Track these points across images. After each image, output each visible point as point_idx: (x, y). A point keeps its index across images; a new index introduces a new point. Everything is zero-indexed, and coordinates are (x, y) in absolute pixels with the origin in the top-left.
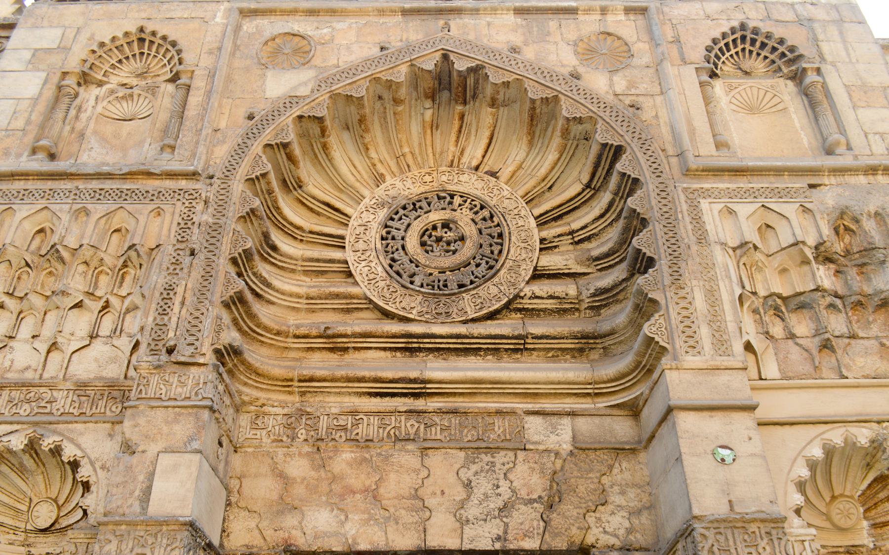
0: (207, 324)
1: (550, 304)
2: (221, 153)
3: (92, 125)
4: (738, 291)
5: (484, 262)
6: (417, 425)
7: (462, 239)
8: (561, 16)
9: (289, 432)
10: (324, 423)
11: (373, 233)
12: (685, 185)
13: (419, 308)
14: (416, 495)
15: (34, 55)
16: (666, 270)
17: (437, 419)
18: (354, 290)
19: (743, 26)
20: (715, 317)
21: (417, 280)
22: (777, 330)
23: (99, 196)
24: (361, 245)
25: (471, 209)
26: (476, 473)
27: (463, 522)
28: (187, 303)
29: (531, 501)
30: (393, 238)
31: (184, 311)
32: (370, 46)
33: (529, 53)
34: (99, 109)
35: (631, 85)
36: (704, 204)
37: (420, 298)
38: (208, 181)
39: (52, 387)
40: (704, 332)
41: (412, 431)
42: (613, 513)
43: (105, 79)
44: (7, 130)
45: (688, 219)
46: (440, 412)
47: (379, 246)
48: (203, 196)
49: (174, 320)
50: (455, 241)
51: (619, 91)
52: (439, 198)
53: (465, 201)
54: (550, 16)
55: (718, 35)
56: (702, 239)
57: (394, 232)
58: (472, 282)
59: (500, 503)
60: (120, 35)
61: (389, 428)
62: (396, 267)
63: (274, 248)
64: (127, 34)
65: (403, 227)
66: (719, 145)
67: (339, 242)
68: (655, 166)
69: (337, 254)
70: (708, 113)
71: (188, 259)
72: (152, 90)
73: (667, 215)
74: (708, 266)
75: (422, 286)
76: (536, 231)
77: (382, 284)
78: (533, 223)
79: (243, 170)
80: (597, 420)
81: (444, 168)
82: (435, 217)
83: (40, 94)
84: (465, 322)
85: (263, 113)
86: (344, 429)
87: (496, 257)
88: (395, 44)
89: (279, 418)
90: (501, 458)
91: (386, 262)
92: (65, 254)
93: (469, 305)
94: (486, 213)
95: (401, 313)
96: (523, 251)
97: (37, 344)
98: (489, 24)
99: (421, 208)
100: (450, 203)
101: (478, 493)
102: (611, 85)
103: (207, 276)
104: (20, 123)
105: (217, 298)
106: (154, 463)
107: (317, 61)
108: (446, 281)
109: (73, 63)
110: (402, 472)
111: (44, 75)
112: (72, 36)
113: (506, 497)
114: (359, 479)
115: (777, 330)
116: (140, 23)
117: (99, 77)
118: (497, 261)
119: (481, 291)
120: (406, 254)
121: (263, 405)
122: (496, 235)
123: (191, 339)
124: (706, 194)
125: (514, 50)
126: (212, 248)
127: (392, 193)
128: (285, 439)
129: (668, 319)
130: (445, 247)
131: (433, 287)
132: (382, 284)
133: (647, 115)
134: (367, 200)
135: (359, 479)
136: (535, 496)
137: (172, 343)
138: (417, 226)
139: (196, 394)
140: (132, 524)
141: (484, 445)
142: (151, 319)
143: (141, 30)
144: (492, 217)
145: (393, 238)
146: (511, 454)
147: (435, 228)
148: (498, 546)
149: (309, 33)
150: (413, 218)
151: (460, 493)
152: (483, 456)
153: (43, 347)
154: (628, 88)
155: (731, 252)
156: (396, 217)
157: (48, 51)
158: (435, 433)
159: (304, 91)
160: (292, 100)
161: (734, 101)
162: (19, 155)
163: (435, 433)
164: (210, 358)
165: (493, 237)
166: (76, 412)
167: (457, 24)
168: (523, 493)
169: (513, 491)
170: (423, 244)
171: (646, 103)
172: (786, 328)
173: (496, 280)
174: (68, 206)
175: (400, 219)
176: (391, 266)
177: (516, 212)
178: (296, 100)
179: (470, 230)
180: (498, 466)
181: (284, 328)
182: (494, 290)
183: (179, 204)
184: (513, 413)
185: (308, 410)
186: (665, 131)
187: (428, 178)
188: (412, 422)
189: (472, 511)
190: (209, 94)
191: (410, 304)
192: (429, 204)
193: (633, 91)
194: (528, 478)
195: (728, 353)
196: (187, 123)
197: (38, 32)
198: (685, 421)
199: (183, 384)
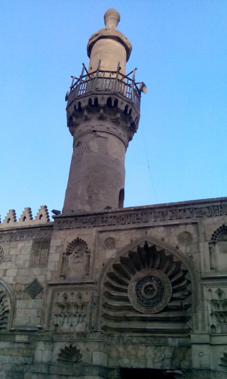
0: (99, 322)
1: (175, 308)
2: (98, 276)
3: (71, 266)
4: (210, 312)
5: (159, 297)
6: (145, 339)
8: (175, 226)
9: (119, 341)
10: (125, 339)
11: (134, 288)
12: (201, 283)
13: (144, 310)
14: (145, 356)
15: (56, 248)
16: (193, 308)
17: (149, 338)
18: (130, 305)
19: (224, 226)
20: (203, 321)
21: (144, 302)
22: (222, 320)
23: (75, 289)
24: (131, 293)
25: (156, 281)
26: (157, 352)
27: (154, 363)
28: (95, 317)
29: (168, 358)
30: (138, 290)
31: (94, 319)
34: (72, 261)
35: (191, 250)
36: (205, 289)
37: (144, 307)
38: (96, 284)
39: (72, 334)
40: (200, 325)
41: (144, 341)
42: (186, 361)
43: (72, 252)
44: (55, 271)
45: (200, 293)
46: (150, 336)
47: (135, 293)
48: (95, 289)
50: (153, 290)
51: (188, 253)
52: (149, 278)
53: (155, 278)
54: (172, 227)
55: (213, 233)
56: (203, 299)
58: (156, 303)
59: (162, 359)
60: (73, 240)
61: (139, 340)
62: (139, 299)
63: (112, 295)
64: (75, 240)
65: (140, 287)
66: (212, 269)
67: (126, 291)
68: (194, 277)
69: (126, 295)
70: (210, 257)
71: (94, 306)
72: (82, 254)
73: (195, 292)
74: (203, 307)
75: (145, 304)
76: (171, 287)
77: (136, 303)
78: (171, 285)
79: (102, 282)
80: (184, 339)
81: (150, 269)
82: (148, 284)
83: (60, 260)
84: (155, 313)
86: (129, 340)
87: (162, 295)
88: (134, 239)
89: (116, 337)
90: (163, 348)
91: (136, 297)
92: (71, 304)
93: (155, 309)
94: (159, 282)
95: (140, 311)
96: (168, 293)
97: (68, 324)
98: (157, 231)
99: (145, 281)
100: (151, 279)
102: (186, 250)
103: (98, 310)
104: (56, 269)
105: (100, 316)
106: (93, 353)
107: (117, 246)
108: (150, 302)
109: (65, 251)
110: (142, 351)
111: (59, 254)
113: (163, 357)
114: (133, 352)
115: (222, 320)
116: (77, 236)
117: (71, 252)
118: (162, 296)
119: (158, 305)
120: (141, 294)
121: (113, 334)
122: (162, 288)
123: (96, 326)
124: (205, 285)
127: (138, 277)
128: (118, 342)
129: (192, 321)
130: (150, 292)
131: (147, 304)
132: (136, 303)
133: (194, 260)
134: (132, 279)
136: (169, 357)
137: (93, 327)
138: (144, 286)
139: (99, 338)
140: (90, 366)
141: (158, 345)
142: (88, 321)
143: (78, 238)
144: (161, 283)
146: (165, 347)
147: (147, 286)
148: (161, 368)
149: (114, 237)
150: (143, 284)
151: (153, 356)
152: (159, 347)
153: (70, 324)
154: (190, 251)
155: (210, 302)
156: (139, 284)
157: (59, 246)
158: (149, 342)
159: (114, 257)
160: (112, 259)
161: (221, 250)
163: (149, 342)
164: (100, 330)
165: (161, 289)
166: (77, 339)
167: (149, 231)
168: (167, 356)
169: (165, 355)
170: (145, 292)
171: (195, 256)
172: (224, 320)
173: (162, 302)
174: (69, 292)
175: (140, 284)
176: (138, 298)
177: (167, 282)
178: (112, 259)
179: (156, 287)
180: (162, 350)
181: (116, 315)
182: (161, 305)
183: (91, 291)
184: (165, 337)
185: (122, 335)
186: (198, 265)
187: (146, 272)
188: (144, 339)
189: (156, 360)
190: (94, 258)
191: (142, 309)
192: (146, 279)
193: (191, 252)
194: (168, 353)
195: (205, 330)
196: (91, 268)
198: (194, 347)
199: (96, 336)
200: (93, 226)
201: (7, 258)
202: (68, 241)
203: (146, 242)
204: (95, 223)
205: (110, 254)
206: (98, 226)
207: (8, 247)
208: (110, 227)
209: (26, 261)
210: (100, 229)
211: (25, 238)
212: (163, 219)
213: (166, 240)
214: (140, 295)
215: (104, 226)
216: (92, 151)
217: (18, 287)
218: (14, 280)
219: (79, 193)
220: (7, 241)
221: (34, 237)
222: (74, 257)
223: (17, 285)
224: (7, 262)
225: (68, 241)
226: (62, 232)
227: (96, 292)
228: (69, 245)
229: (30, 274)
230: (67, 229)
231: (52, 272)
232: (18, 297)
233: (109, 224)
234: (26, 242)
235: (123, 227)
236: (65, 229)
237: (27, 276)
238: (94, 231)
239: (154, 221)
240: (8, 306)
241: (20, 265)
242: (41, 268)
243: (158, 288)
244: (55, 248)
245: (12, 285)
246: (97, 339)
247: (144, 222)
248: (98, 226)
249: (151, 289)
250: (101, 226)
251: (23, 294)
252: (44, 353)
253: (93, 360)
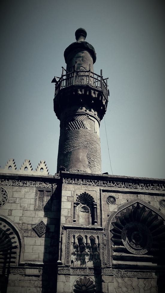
10: (122, 273)
17: (139, 273)
28: (106, 255)
29: (154, 287)
32: (125, 200)
33: (152, 204)
41: (136, 274)
49: (105, 259)
64: (83, 193)
84: (143, 254)
85: (110, 215)
88: (129, 200)
101: (147, 285)
104: (69, 215)
111: (70, 203)
112: (73, 193)
113: (151, 286)
114: (129, 283)
116: (85, 191)
125: (149, 202)
126: (108, 245)
135: (129, 283)
136: (155, 286)
143: (85, 193)
146: (151, 279)
159: (116, 210)
162: (72, 223)
189: (146, 289)
197: (67, 191)
200: (97, 185)
201: (11, 200)
202: (77, 193)
203: (138, 203)
204: (98, 183)
205: (113, 208)
206: (100, 186)
207: (11, 190)
208: (110, 187)
210: (102, 188)
211: (28, 185)
212: (148, 188)
213: (152, 204)
215: (106, 186)
216: (87, 128)
217: (25, 227)
218: (20, 220)
219: (80, 157)
220: (9, 185)
222: (81, 207)
224: (12, 203)
225: (77, 193)
227: (105, 236)
228: (78, 197)
229: (36, 216)
230: (75, 184)
231: (66, 216)
232: (25, 234)
233: (109, 186)
235: (119, 189)
236: (73, 184)
238: (97, 189)
239: (141, 189)
240: (15, 242)
244: (66, 198)
245: (19, 224)
246: (110, 273)
247: (135, 188)
248: (100, 186)
250: (103, 186)
251: (30, 232)
252: (66, 284)
253: (109, 289)
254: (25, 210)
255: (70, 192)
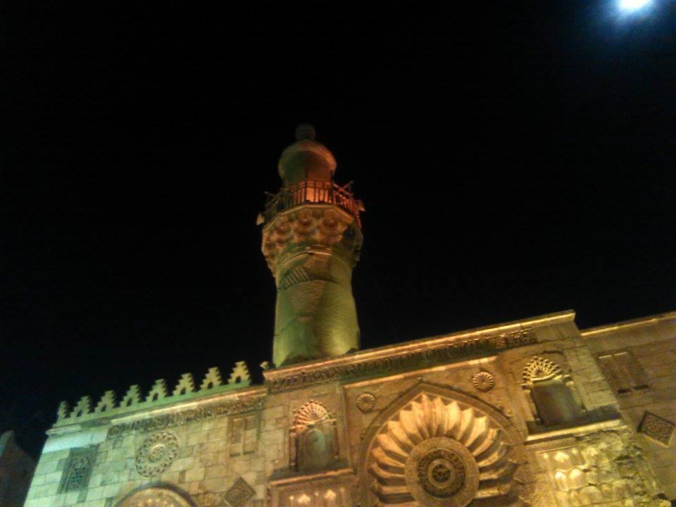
7: (449, 472)
24: (412, 481)
30: (423, 475)
57: (423, 473)
82: (437, 462)
94: (454, 458)
104: (281, 455)
138: (431, 468)
145: (423, 475)
147: (437, 468)
157: (281, 418)
170: (434, 476)
173: (466, 489)
207: (185, 433)
209: (219, 452)
214: (426, 483)
221: (229, 413)
223: (206, 496)
226: (283, 396)
234: (216, 420)
237: (223, 478)
241: (208, 460)
242: (248, 460)
243: (455, 467)
249: (443, 470)
254: (210, 466)
255: (280, 409)
